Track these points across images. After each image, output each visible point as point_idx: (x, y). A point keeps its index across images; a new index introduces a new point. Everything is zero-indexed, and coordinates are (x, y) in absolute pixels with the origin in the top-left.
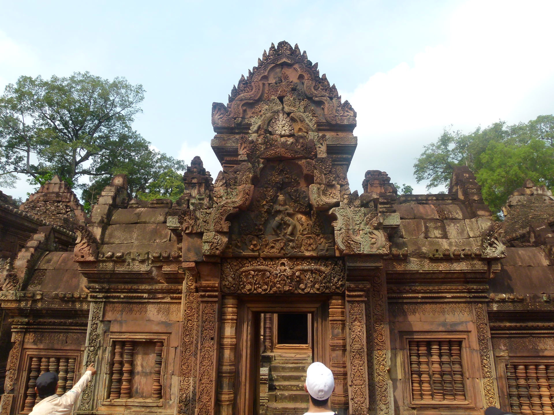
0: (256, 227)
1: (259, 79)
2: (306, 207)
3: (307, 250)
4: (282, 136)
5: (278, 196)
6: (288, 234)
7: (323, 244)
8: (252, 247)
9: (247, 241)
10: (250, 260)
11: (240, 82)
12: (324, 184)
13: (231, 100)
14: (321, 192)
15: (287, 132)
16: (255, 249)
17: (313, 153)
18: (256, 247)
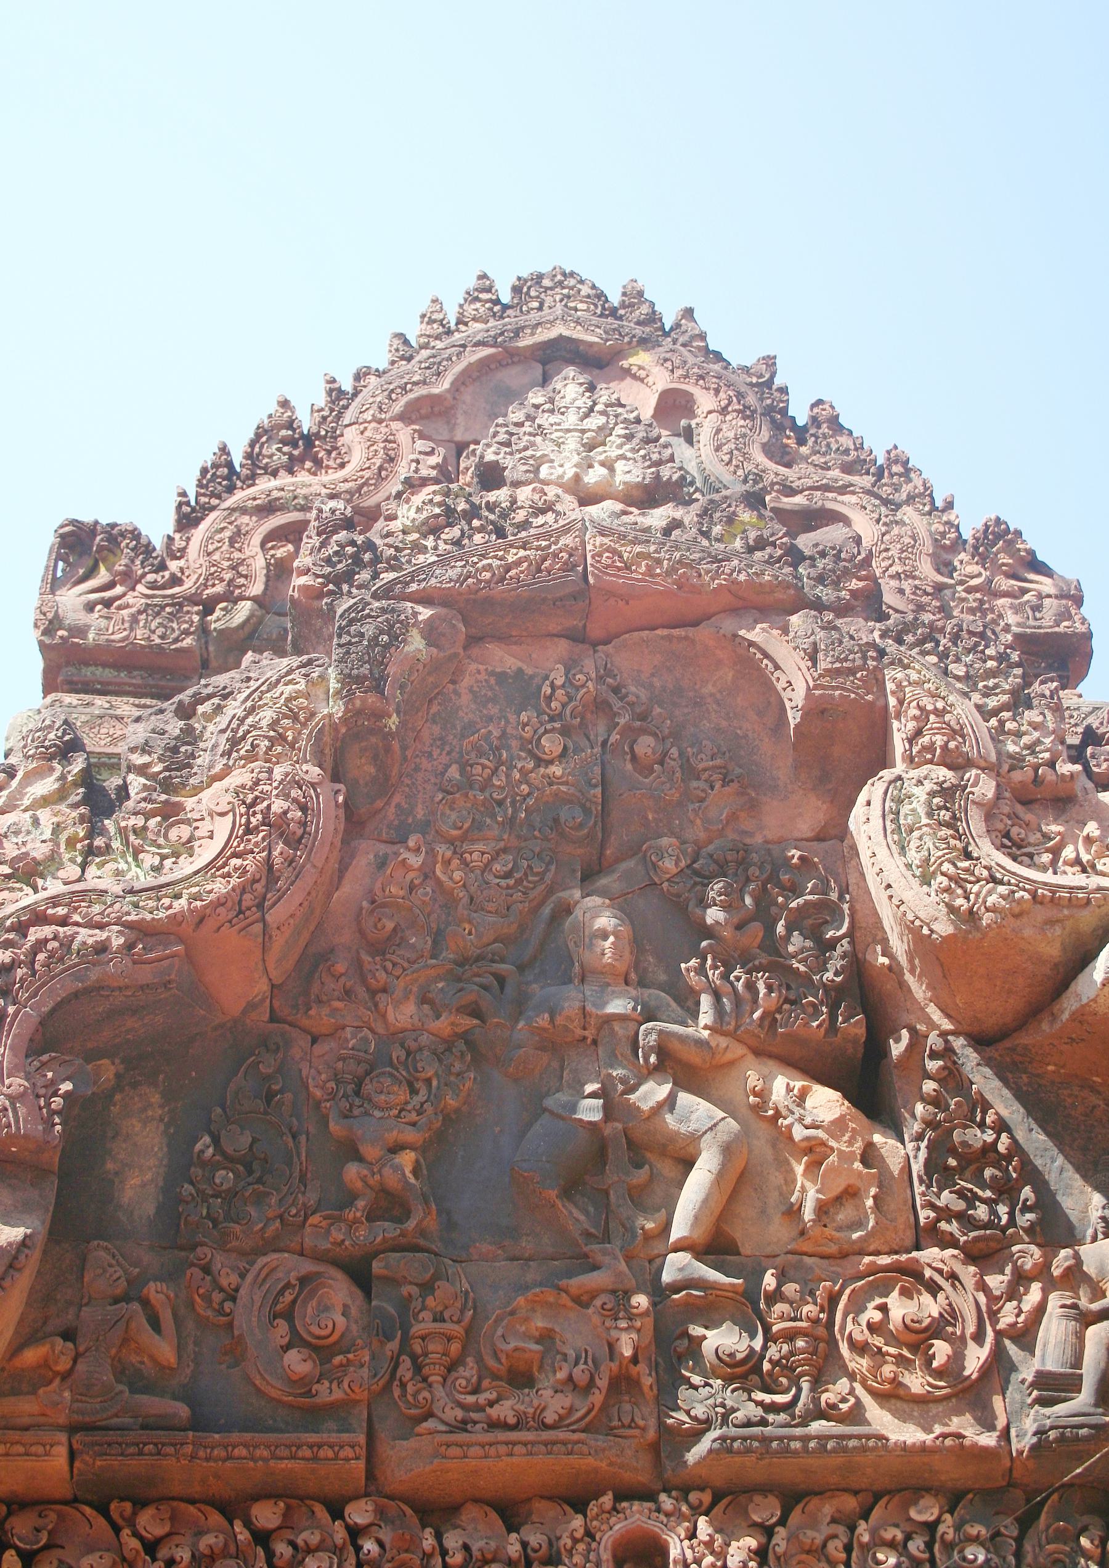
0: (352, 1171)
1: (398, 408)
2: (835, 996)
3: (892, 1396)
4: (586, 500)
5: (567, 909)
6: (679, 1230)
7: (1054, 1330)
8: (297, 1362)
9: (247, 1316)
10: (266, 1515)
11: (262, 434)
12: (988, 768)
13: (188, 518)
14: (976, 823)
15: (630, 473)
16: (327, 1393)
17: (855, 584)
18: (335, 1376)
